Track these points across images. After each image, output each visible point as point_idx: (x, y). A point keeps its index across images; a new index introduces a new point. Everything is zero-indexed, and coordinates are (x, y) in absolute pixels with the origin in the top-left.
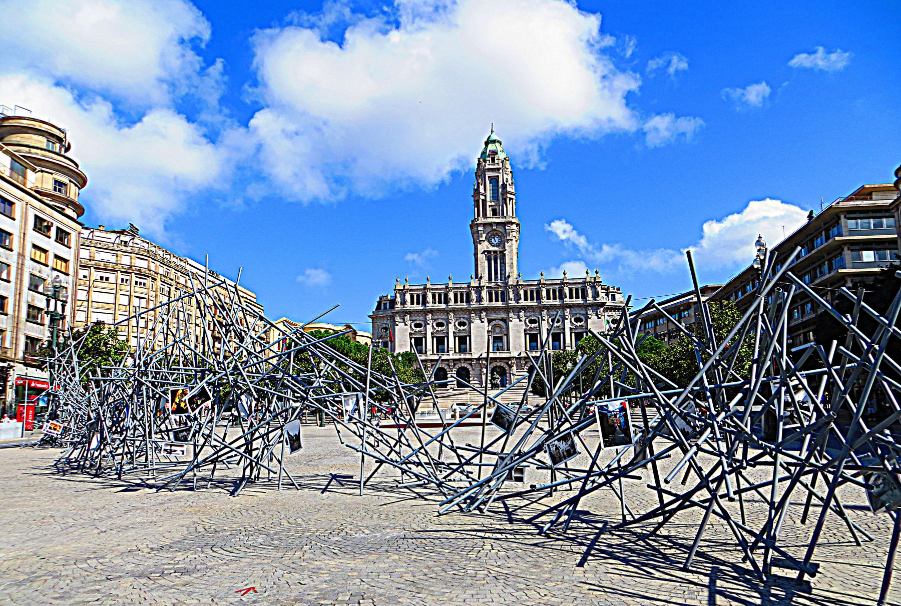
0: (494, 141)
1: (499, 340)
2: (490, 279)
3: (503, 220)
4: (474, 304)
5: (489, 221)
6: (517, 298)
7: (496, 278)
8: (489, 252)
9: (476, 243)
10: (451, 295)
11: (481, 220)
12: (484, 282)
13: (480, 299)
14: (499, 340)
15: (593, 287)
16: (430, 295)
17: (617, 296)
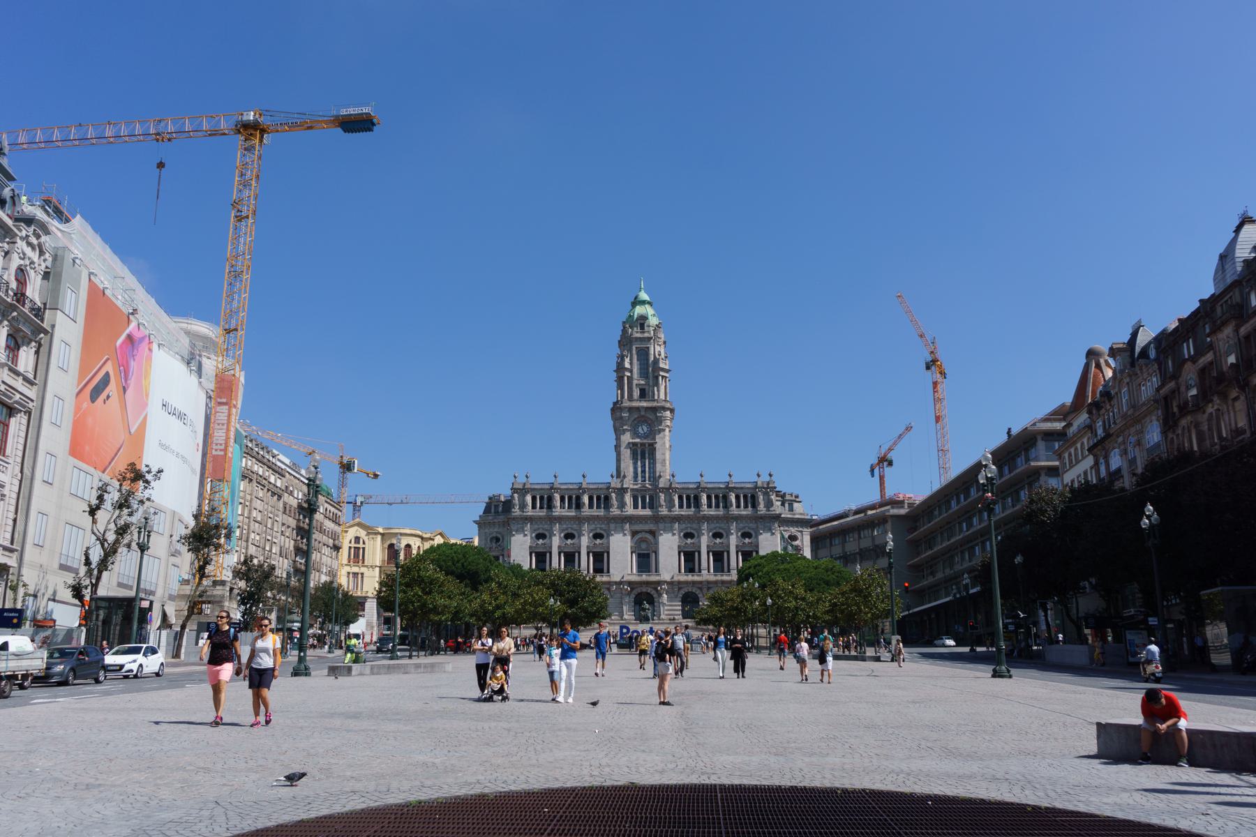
0: (643, 302)
1: (645, 560)
2: (636, 477)
3: (655, 404)
4: (615, 511)
5: (635, 404)
6: (670, 505)
7: (643, 477)
8: (635, 444)
9: (618, 432)
10: (586, 499)
11: (626, 404)
13: (622, 505)
14: (645, 560)
15: (766, 494)
16: (557, 497)
17: (795, 505)
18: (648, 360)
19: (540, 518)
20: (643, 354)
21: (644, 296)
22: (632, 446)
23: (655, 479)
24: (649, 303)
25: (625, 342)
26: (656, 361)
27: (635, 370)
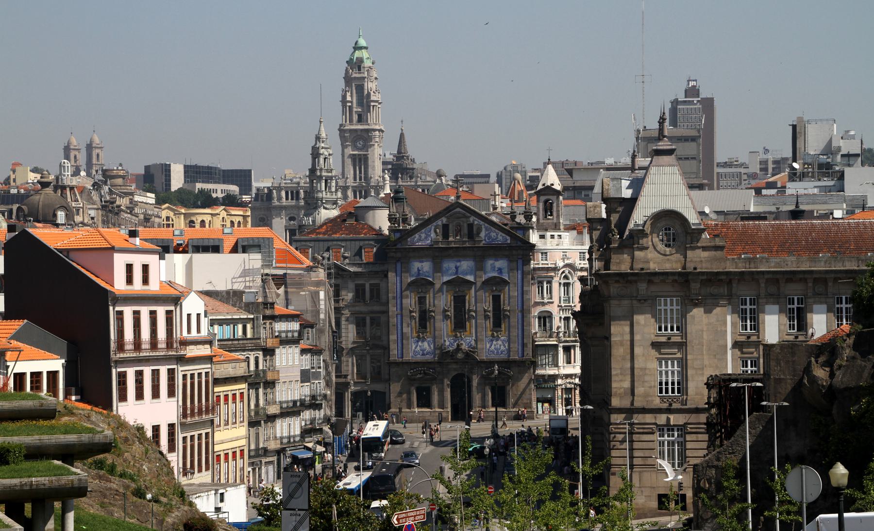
0: (361, 48)
2: (355, 179)
7: (360, 179)
9: (344, 147)
12: (350, 182)
18: (363, 93)
19: (292, 207)
20: (360, 88)
21: (362, 42)
22: (353, 157)
23: (367, 179)
24: (366, 48)
25: (348, 80)
26: (369, 95)
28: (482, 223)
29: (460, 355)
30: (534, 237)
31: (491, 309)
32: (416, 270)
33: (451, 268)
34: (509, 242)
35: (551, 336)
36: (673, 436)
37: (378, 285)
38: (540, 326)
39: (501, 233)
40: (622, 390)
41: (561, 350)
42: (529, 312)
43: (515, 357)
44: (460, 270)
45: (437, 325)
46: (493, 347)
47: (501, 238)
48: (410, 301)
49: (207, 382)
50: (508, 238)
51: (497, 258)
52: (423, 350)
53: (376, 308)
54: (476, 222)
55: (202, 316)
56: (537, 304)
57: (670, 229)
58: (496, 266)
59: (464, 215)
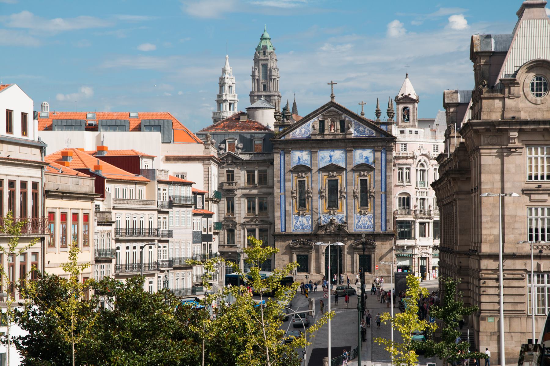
0: (266, 39)
3: (269, 94)
20: (265, 66)
21: (267, 35)
24: (270, 39)
25: (256, 61)
27: (261, 76)
28: (352, 119)
29: (333, 229)
30: (395, 131)
31: (359, 190)
32: (297, 158)
33: (325, 157)
34: (374, 135)
35: (409, 213)
36: (543, 282)
37: (266, 171)
38: (400, 205)
39: (367, 128)
40: (492, 237)
41: (417, 225)
42: (392, 193)
43: (378, 230)
44: (333, 159)
45: (314, 204)
46: (361, 222)
47: (368, 132)
48: (292, 184)
49: (35, 196)
50: (374, 131)
51: (364, 148)
52: (302, 225)
53: (264, 190)
54: (347, 119)
55: (30, 117)
56: (397, 186)
57: (541, 79)
58: (361, 155)
59: (337, 112)
